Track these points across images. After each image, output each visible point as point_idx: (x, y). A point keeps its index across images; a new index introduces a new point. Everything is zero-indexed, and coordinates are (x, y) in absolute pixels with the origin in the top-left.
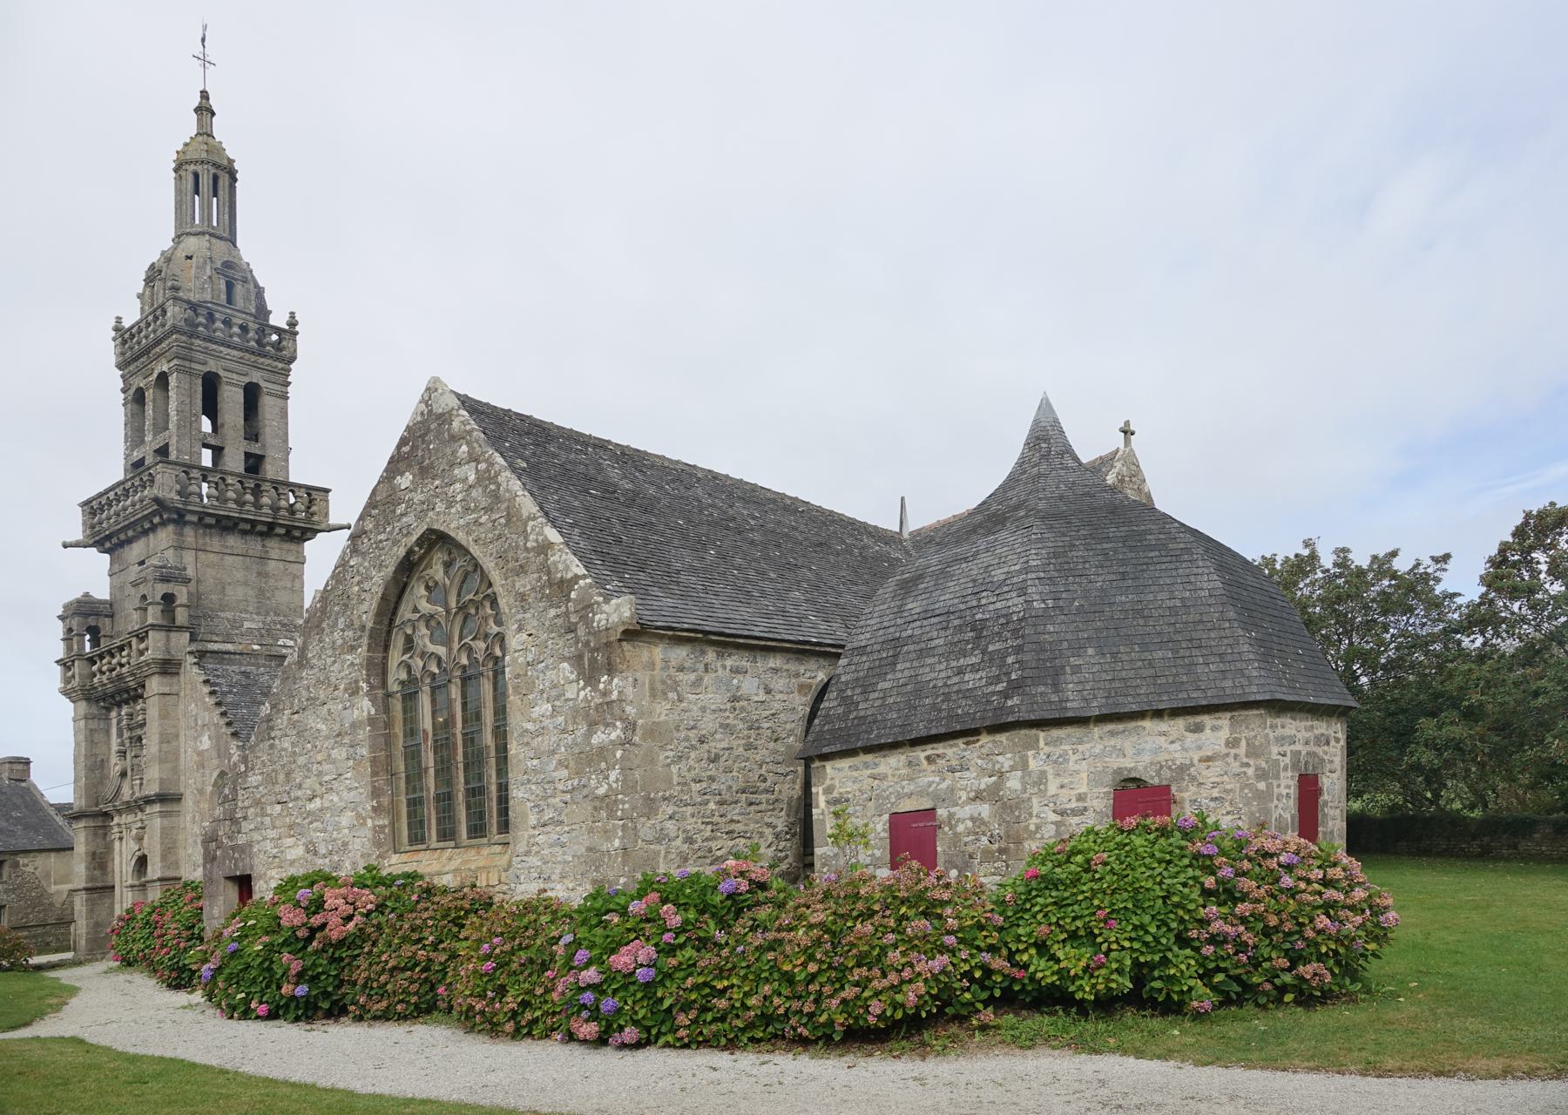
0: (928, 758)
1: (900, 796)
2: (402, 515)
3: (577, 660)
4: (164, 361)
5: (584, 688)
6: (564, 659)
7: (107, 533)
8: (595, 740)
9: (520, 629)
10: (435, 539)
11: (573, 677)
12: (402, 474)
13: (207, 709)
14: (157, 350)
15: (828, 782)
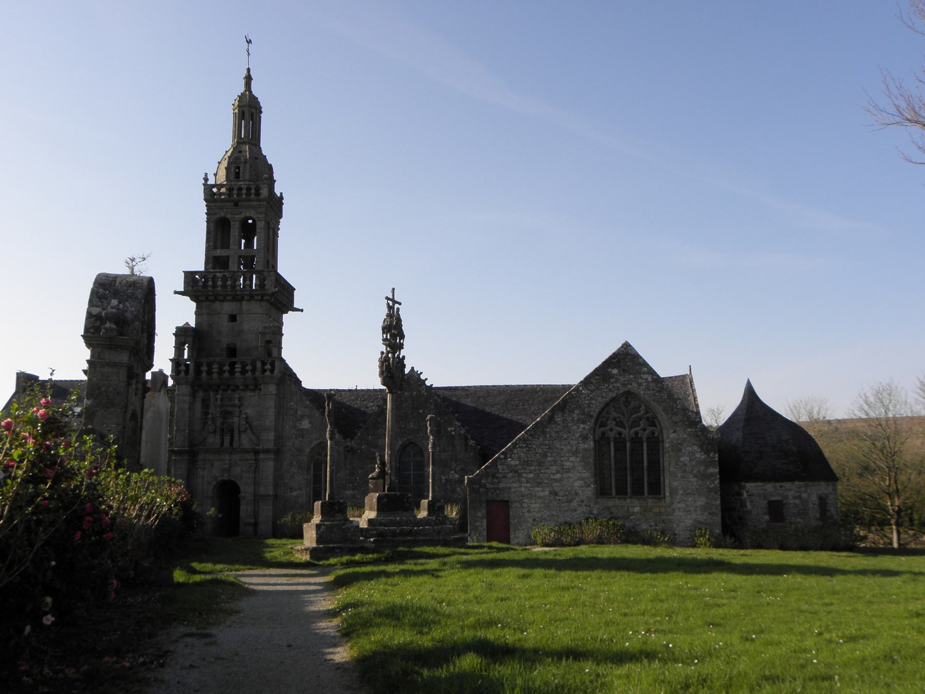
2: (613, 382)
3: (701, 446)
5: (704, 455)
6: (696, 445)
9: (674, 432)
10: (629, 394)
11: (699, 450)
12: (613, 368)
14: (245, 203)
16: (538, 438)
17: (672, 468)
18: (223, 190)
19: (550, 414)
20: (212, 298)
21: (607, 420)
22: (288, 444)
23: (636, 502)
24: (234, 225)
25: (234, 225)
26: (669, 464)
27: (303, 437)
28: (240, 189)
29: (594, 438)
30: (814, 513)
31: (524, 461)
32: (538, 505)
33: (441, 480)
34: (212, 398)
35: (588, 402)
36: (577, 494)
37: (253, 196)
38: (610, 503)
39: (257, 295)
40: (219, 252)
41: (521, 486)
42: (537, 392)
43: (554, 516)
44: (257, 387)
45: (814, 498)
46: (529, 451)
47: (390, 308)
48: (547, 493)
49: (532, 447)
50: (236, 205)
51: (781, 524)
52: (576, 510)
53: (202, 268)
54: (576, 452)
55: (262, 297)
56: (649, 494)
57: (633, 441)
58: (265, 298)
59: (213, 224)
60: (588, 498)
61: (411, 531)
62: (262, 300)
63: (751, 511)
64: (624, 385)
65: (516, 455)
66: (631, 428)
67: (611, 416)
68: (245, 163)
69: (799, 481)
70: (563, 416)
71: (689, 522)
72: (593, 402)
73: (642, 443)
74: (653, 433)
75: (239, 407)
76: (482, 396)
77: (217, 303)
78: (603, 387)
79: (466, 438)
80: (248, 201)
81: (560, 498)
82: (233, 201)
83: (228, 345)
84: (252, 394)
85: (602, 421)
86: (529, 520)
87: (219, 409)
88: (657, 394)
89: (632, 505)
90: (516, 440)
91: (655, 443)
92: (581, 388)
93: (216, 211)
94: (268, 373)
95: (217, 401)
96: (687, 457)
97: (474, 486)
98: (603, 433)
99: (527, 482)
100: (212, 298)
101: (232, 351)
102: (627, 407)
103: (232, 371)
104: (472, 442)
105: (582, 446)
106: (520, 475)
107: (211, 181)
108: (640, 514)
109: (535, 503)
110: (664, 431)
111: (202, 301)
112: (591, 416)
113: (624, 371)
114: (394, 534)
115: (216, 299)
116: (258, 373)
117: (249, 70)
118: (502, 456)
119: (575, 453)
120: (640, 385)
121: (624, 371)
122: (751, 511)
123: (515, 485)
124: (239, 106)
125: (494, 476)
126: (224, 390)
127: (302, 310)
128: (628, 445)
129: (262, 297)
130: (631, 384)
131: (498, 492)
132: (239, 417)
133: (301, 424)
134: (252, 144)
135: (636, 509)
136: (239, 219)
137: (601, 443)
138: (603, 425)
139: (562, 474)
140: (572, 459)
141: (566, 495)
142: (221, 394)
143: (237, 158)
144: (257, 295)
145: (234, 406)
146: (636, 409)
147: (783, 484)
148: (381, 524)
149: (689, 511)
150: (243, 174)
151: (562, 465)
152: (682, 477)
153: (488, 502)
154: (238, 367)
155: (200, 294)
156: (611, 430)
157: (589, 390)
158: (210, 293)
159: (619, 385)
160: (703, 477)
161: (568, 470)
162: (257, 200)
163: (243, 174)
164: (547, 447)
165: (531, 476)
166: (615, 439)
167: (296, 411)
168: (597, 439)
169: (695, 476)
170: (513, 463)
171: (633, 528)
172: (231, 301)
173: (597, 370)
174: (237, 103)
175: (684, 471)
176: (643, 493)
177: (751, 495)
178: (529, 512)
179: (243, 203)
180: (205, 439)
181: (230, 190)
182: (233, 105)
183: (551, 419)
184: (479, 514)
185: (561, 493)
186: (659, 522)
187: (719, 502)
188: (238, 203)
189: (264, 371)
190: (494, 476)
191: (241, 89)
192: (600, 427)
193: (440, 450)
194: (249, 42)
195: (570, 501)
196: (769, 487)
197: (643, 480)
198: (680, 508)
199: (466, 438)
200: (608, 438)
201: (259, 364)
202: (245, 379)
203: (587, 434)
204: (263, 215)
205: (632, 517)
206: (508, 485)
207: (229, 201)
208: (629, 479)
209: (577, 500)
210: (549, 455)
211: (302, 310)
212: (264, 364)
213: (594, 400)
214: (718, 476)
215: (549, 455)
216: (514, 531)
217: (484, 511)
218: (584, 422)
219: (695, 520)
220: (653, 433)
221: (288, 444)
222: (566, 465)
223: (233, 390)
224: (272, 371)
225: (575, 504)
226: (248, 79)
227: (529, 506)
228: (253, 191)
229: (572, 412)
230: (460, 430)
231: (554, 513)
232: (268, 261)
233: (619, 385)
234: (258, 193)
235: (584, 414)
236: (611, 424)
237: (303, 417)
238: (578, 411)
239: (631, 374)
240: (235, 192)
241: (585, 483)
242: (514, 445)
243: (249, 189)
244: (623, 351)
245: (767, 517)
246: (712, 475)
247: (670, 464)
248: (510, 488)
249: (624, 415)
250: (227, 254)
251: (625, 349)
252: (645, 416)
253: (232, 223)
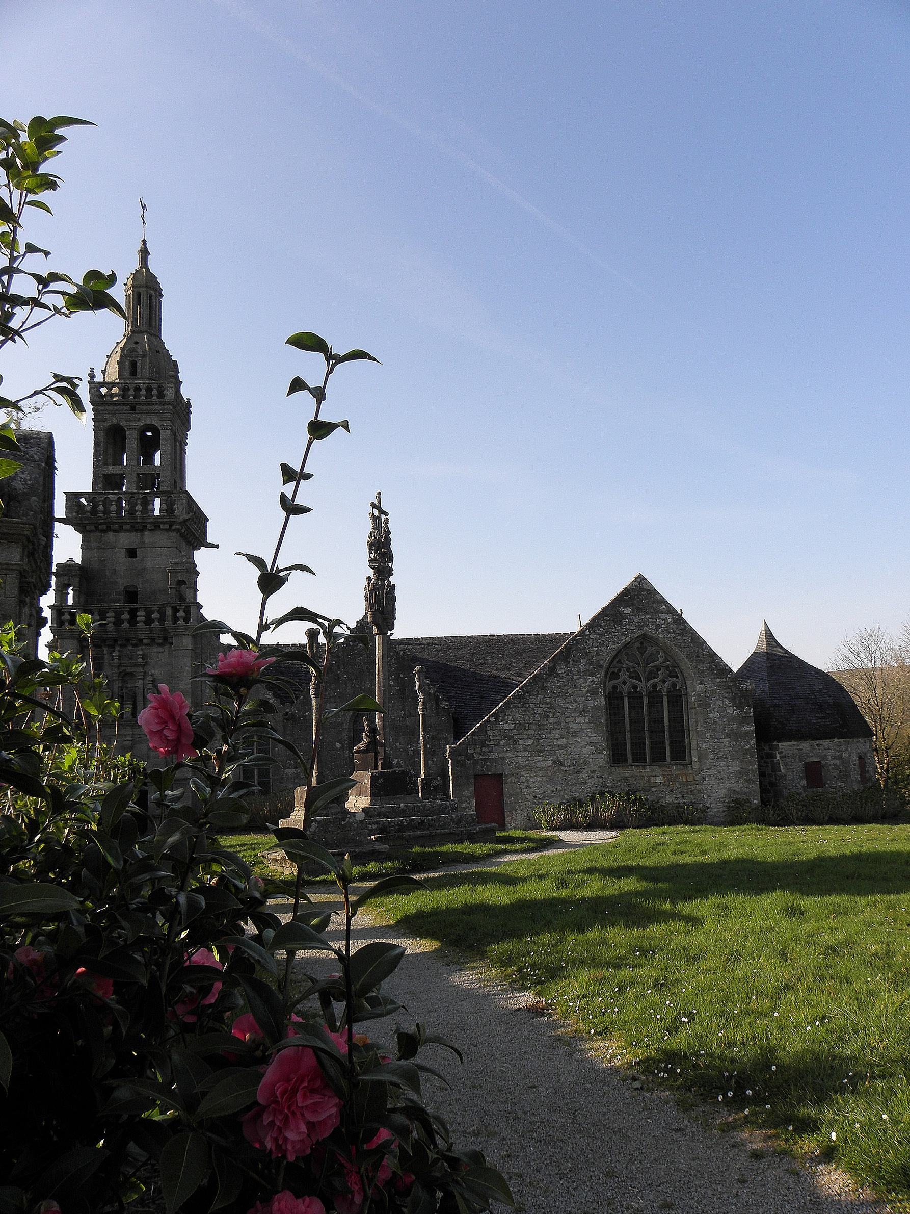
0: (817, 745)
1: (808, 756)
3: (733, 700)
6: (726, 698)
8: (743, 729)
9: (701, 683)
10: (645, 639)
14: (145, 407)
15: (780, 750)
16: (537, 695)
17: (699, 726)
18: (115, 390)
19: (551, 664)
20: (105, 527)
21: (620, 671)
23: (657, 770)
26: (694, 721)
28: (138, 389)
29: (605, 693)
30: (856, 776)
31: (520, 724)
32: (539, 779)
33: (407, 751)
34: (106, 656)
35: (596, 648)
36: (586, 763)
37: (155, 398)
38: (627, 773)
39: (164, 523)
40: (111, 469)
41: (517, 756)
42: (506, 643)
43: (559, 791)
44: (166, 640)
45: (855, 757)
46: (525, 711)
47: (375, 519)
48: (550, 763)
49: (529, 707)
50: (133, 409)
51: (820, 790)
52: (585, 783)
53: (89, 488)
54: (584, 711)
55: (171, 526)
56: (633, 761)
57: (649, 695)
58: (174, 527)
59: (102, 433)
60: (600, 767)
61: (423, 821)
62: (170, 529)
63: (785, 776)
64: (639, 627)
65: (511, 717)
66: (648, 679)
67: (624, 666)
68: (144, 356)
69: (838, 739)
70: (566, 667)
71: (722, 792)
72: (603, 649)
73: (662, 697)
74: (674, 685)
75: (143, 666)
76: (441, 650)
77: (111, 534)
78: (614, 630)
79: (437, 700)
80: (149, 404)
81: (566, 769)
82: (128, 404)
83: (126, 587)
84: (160, 649)
85: (613, 672)
86: (528, 797)
87: (116, 670)
88: (678, 638)
89: (654, 774)
90: (510, 698)
91: (677, 698)
92: (587, 632)
93: (107, 416)
94: (181, 622)
95: (113, 660)
96: (717, 714)
97: (459, 758)
98: (615, 687)
99: (525, 750)
100: (105, 527)
101: (132, 595)
102: (642, 654)
103: (133, 620)
104: (444, 704)
105: (591, 703)
106: (515, 742)
107: (99, 378)
108: (664, 785)
109: (535, 776)
110: (688, 683)
111: (90, 531)
112: (601, 667)
113: (639, 610)
114: (401, 828)
115: (109, 529)
116: (168, 623)
117: (144, 241)
118: (492, 719)
119: (583, 712)
120: (658, 626)
121: (639, 610)
122: (785, 776)
123: (509, 754)
124: (133, 286)
125: (483, 745)
126: (123, 646)
127: (217, 546)
128: (645, 700)
129: (171, 526)
130: (648, 626)
131: (488, 764)
132: (143, 679)
134: (152, 335)
135: (659, 779)
136: (138, 427)
137: (613, 699)
138: (615, 676)
139: (567, 738)
140: (580, 720)
141: (574, 765)
142: (119, 651)
143: (133, 350)
144: (164, 523)
145: (136, 665)
146: (653, 657)
147: (821, 742)
148: (380, 815)
149: (722, 779)
150: (142, 370)
151: (568, 728)
152: (712, 737)
153: (476, 777)
154: (141, 615)
155: (87, 522)
156: (624, 683)
157: (597, 634)
158: (102, 521)
159: (633, 627)
160: (736, 736)
161: (575, 734)
162: (161, 404)
163: (142, 370)
164: (549, 706)
165: (530, 742)
166: (629, 693)
168: (607, 694)
169: (727, 736)
170: (506, 727)
171: (657, 802)
172: (126, 531)
173: (605, 609)
174: (130, 282)
175: (714, 730)
176: (665, 760)
177: (785, 757)
178: (528, 787)
179: (141, 407)
181: (125, 390)
182: (125, 285)
183: (551, 671)
184: (466, 793)
185: (567, 763)
186: (687, 793)
187: (756, 767)
189: (176, 619)
190: (483, 745)
191: (137, 265)
192: (611, 680)
193: (404, 714)
194: (144, 207)
195: (580, 772)
196: (805, 746)
197: (664, 743)
198: (710, 775)
199: (437, 700)
200: (621, 693)
201: (169, 611)
202: (151, 630)
203: (597, 689)
204: (170, 423)
205: (654, 789)
206: (500, 755)
207: (124, 404)
208: (647, 742)
209: (586, 770)
210: (551, 715)
211: (217, 546)
212: (175, 610)
213: (603, 646)
214: (754, 735)
215: (551, 715)
216: (511, 812)
217: (472, 788)
218: (592, 674)
219: (729, 790)
220: (674, 685)
222: (572, 728)
223: (134, 646)
224: (187, 620)
225: (584, 775)
226: (144, 253)
227: (528, 780)
228: (155, 392)
229: (578, 661)
230: (430, 689)
231: (559, 788)
232: (175, 482)
233: (633, 627)
234: (161, 395)
235: (592, 663)
236: (624, 675)
238: (585, 660)
239: (647, 614)
240: (131, 392)
241: (597, 749)
242: (507, 704)
243: (149, 389)
244: (636, 586)
245: (804, 782)
246: (747, 733)
247: (697, 722)
248: (504, 758)
249: (639, 664)
251: (639, 583)
252: (665, 664)
253: (128, 432)
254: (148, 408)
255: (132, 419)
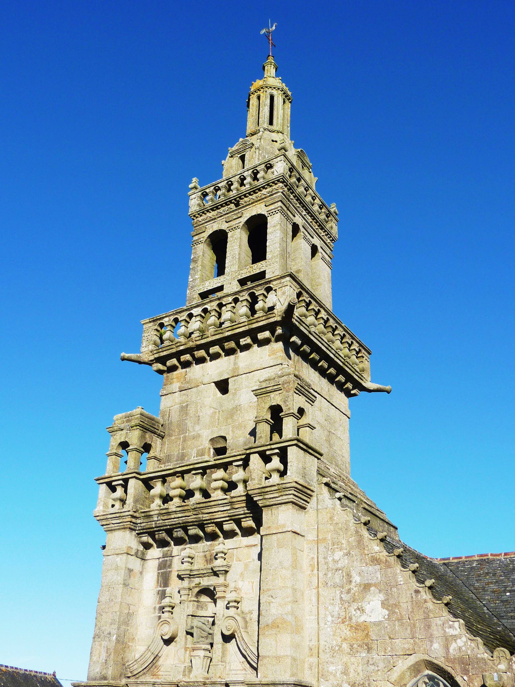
4: (263, 205)
7: (182, 348)
13: (375, 561)
22: (332, 668)
24: (232, 237)
25: (232, 237)
27: (369, 650)
82: (231, 202)
133: (361, 610)
136: (241, 224)
144: (262, 329)
167: (349, 575)
180: (156, 657)
188: (238, 201)
221: (332, 668)
224: (283, 473)
237: (366, 587)
250: (219, 285)
254: (254, 196)
255: (235, 217)
